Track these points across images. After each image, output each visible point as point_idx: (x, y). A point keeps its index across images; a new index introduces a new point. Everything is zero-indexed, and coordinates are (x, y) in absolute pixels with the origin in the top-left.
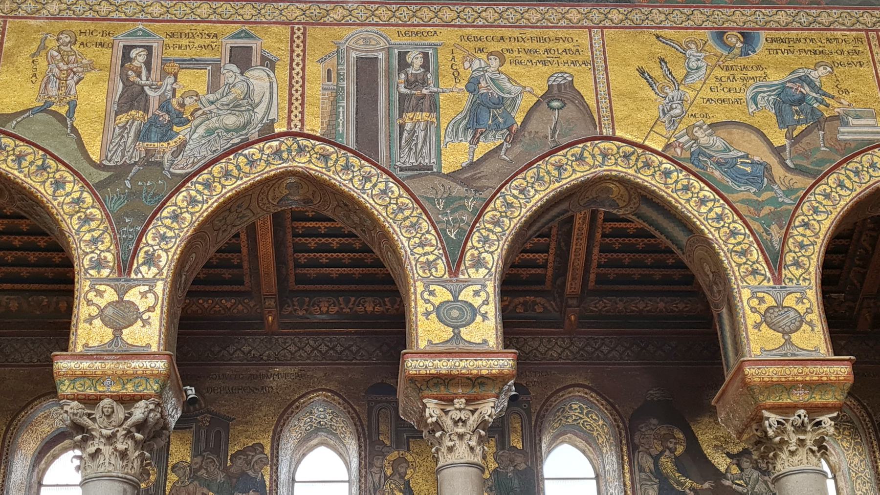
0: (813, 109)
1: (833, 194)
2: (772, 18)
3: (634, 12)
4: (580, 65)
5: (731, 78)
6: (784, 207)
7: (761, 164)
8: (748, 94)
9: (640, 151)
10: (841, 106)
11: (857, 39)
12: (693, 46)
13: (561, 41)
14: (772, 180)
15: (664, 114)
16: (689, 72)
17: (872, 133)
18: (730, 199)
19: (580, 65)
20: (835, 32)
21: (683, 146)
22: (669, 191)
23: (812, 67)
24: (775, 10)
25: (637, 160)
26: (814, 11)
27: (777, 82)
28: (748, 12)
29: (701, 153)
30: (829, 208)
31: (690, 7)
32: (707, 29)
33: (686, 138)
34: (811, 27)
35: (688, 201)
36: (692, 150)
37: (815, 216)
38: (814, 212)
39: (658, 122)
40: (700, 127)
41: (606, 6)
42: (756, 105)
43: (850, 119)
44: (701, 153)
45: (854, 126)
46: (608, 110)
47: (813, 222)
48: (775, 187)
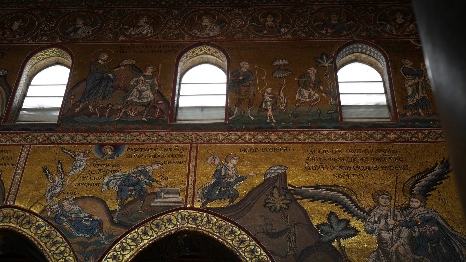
0: (142, 189)
1: (139, 238)
2: (136, 138)
3: (54, 135)
4: (9, 166)
5: (98, 172)
6: (103, 246)
7: (97, 221)
8: (105, 180)
9: (27, 214)
10: (160, 186)
11: (184, 148)
12: (82, 154)
13: (4, 152)
14: (101, 231)
15: (49, 192)
16: (73, 168)
17: (174, 202)
18: (70, 242)
19: (9, 166)
20: (172, 145)
21: (53, 210)
22: (36, 238)
23: (151, 164)
24: (139, 133)
25: (23, 219)
26: (163, 133)
27: (125, 174)
28: (122, 134)
29: (63, 214)
30: (132, 247)
31: (89, 132)
32: (94, 144)
33: (57, 206)
34: (158, 142)
35: (46, 243)
36: (58, 213)
37: (122, 252)
38: (122, 250)
39: (44, 197)
40: (68, 200)
41: (38, 133)
42: (108, 187)
43: (163, 194)
44: (63, 214)
45: (164, 198)
46: (16, 190)
47: (119, 255)
48: (101, 234)
